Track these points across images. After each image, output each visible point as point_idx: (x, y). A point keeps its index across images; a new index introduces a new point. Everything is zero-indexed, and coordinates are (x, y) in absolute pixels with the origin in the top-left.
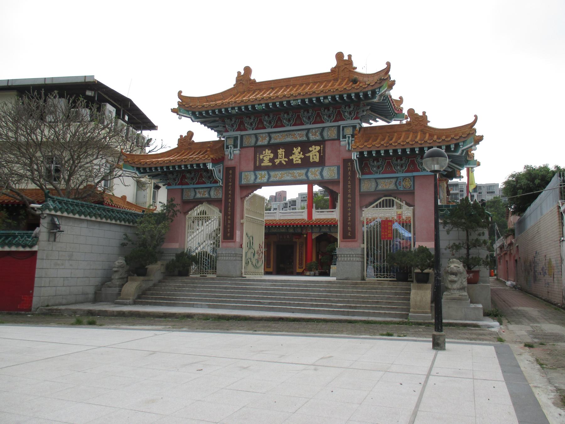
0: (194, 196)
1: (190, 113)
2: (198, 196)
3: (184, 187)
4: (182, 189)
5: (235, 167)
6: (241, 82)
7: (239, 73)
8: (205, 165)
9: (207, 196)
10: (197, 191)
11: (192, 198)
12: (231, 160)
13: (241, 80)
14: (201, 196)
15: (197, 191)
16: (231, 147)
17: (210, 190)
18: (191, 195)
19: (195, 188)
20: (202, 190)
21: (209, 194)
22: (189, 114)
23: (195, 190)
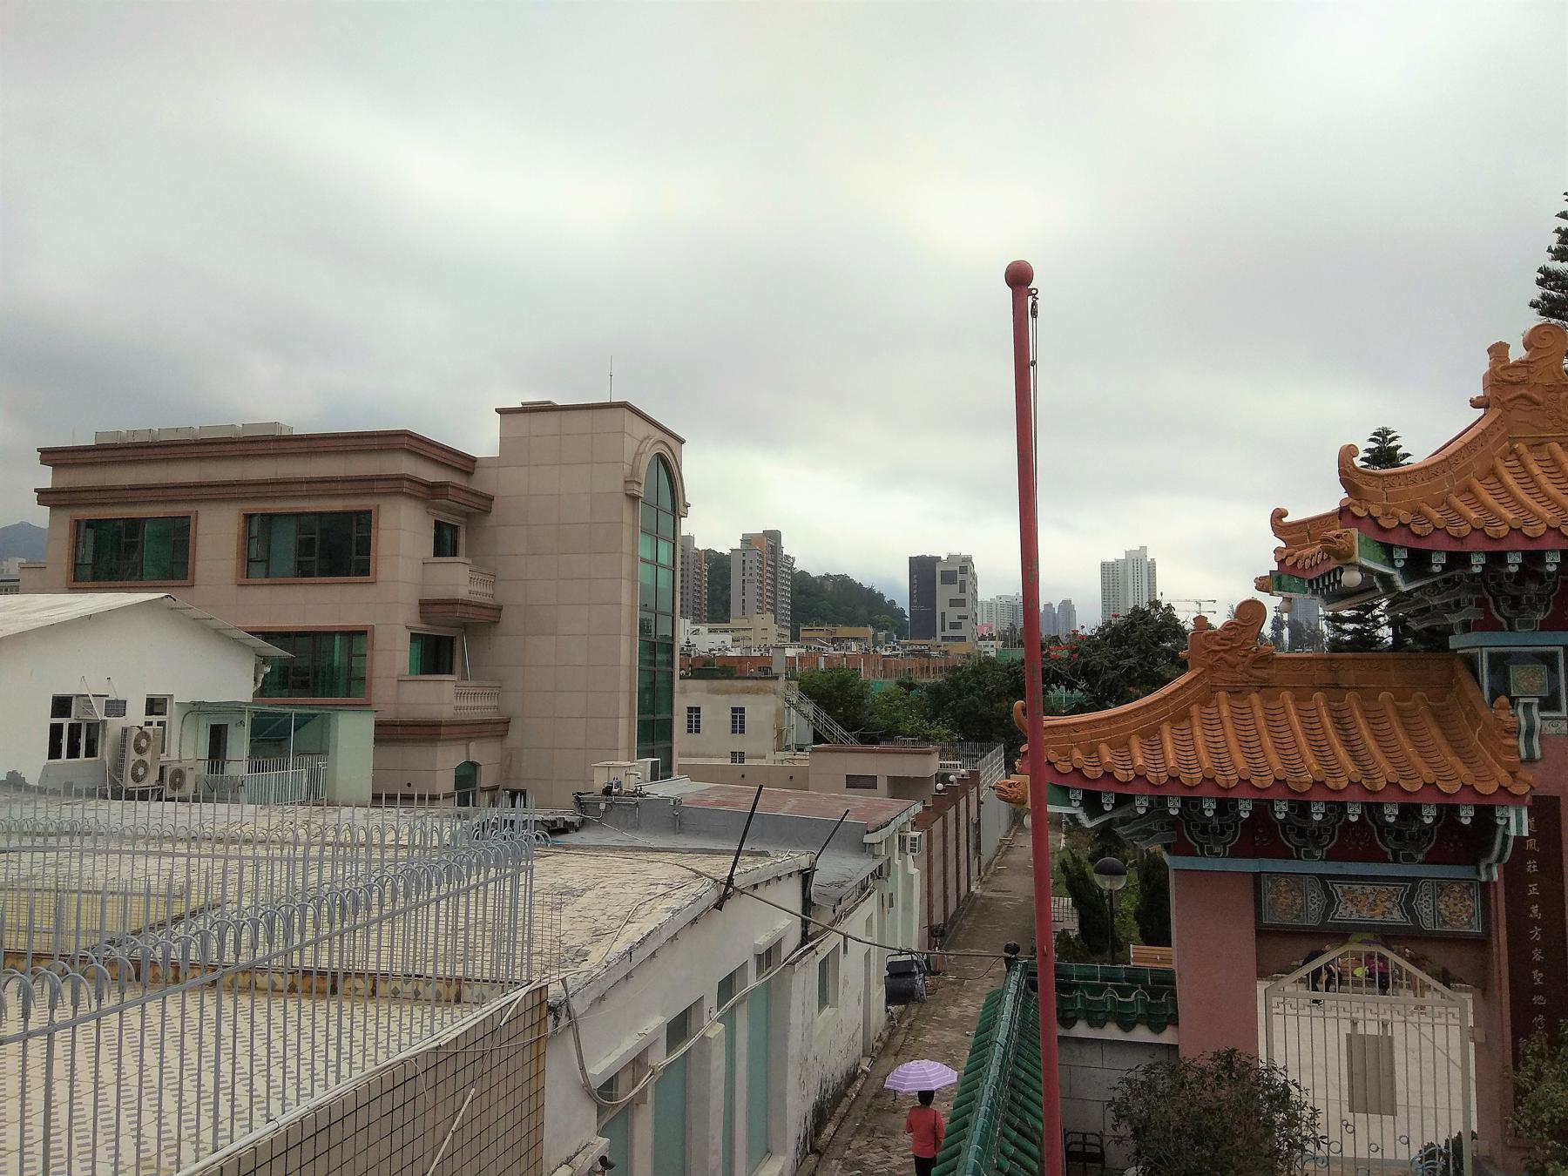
0: (1326, 915)
1: (1401, 555)
2: (1346, 912)
3: (1270, 865)
4: (1257, 877)
5: (1558, 798)
6: (1524, 391)
7: (1498, 351)
8: (1485, 814)
9: (1397, 917)
10: (1338, 889)
11: (1312, 921)
12: (1531, 759)
13: (1522, 382)
14: (1366, 914)
15: (1338, 889)
16: (1527, 706)
17: (1413, 890)
18: (1310, 910)
19: (1322, 877)
20: (1368, 889)
21: (1410, 911)
22: (1392, 564)
23: (1325, 888)
